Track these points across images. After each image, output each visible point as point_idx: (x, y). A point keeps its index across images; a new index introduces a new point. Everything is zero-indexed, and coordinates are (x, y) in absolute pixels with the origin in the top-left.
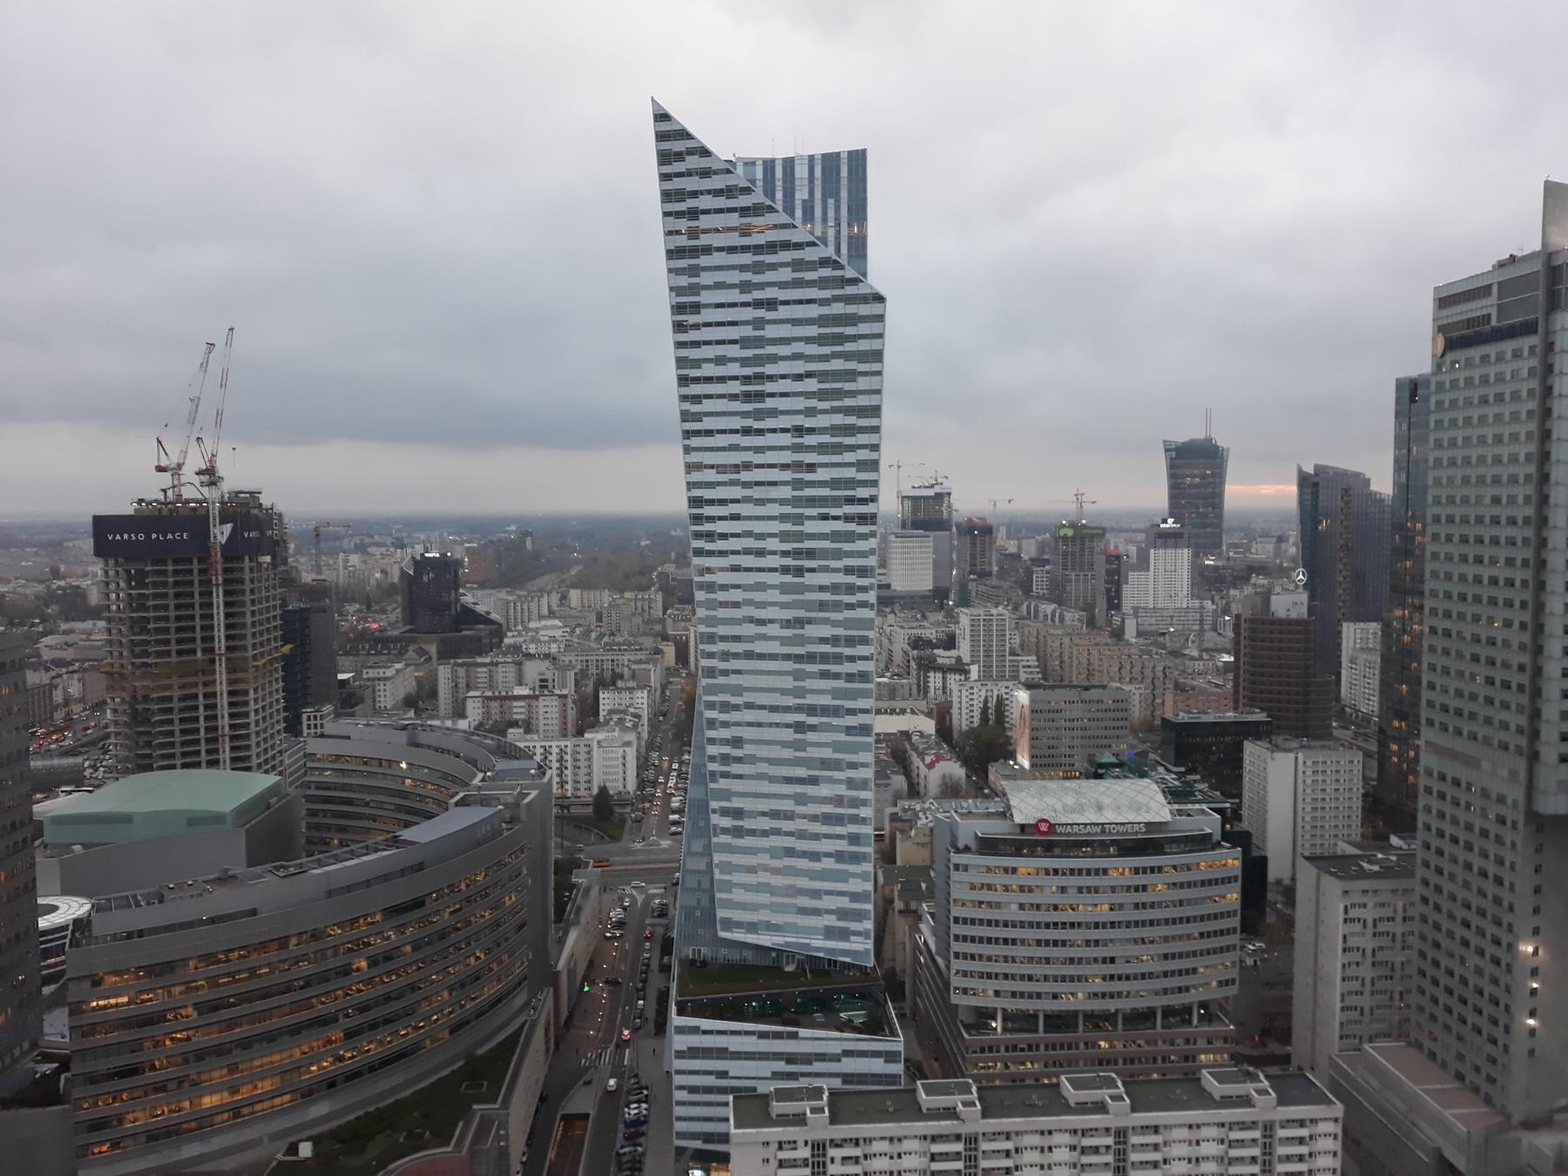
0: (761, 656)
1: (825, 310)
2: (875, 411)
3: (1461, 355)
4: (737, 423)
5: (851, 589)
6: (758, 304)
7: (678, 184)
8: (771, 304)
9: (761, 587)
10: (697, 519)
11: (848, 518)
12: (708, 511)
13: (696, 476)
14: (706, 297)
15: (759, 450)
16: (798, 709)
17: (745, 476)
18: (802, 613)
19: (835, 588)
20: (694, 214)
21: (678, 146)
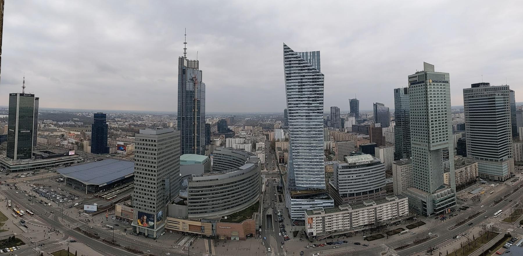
0: (302, 137)
1: (313, 77)
2: (323, 94)
3: (413, 86)
4: (297, 96)
5: (319, 125)
6: (301, 76)
7: (288, 56)
8: (304, 76)
9: (302, 125)
10: (290, 113)
11: (318, 113)
12: (292, 112)
13: (290, 106)
14: (292, 75)
15: (302, 101)
16: (309, 146)
17: (299, 105)
18: (310, 130)
19: (316, 125)
20: (290, 61)
21: (288, 50)
